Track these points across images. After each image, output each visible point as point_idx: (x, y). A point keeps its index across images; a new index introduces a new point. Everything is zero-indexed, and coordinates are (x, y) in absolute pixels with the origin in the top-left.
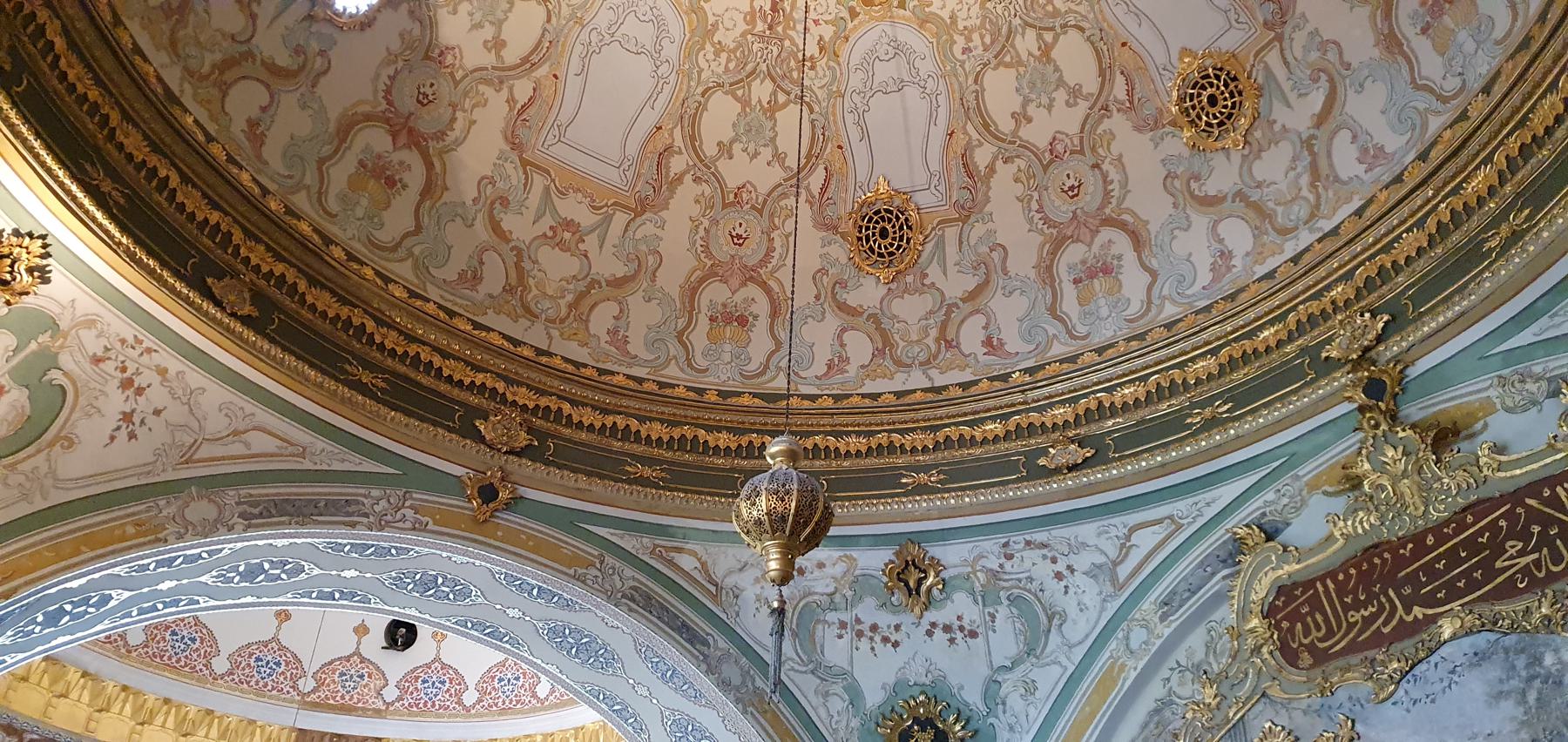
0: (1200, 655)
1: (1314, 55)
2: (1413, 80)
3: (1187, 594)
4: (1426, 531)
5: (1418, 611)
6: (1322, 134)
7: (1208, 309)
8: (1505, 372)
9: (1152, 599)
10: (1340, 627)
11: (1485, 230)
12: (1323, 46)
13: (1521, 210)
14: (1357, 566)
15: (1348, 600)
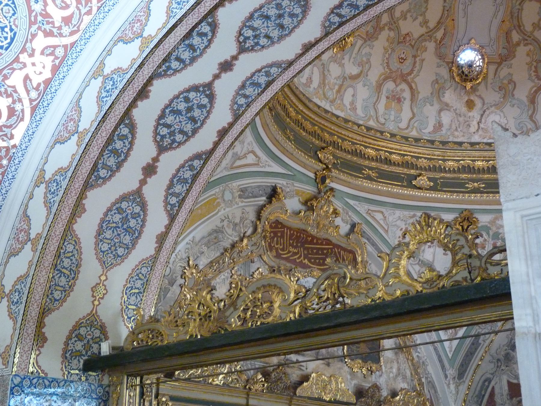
0: (237, 220)
1: (364, 59)
2: (375, 104)
3: (250, 195)
4: (317, 238)
5: (306, 261)
6: (348, 82)
7: (304, 95)
8: (345, 207)
9: (239, 183)
10: (287, 249)
11: (366, 167)
12: (368, 61)
13: (376, 172)
14: (297, 233)
15: (291, 242)
